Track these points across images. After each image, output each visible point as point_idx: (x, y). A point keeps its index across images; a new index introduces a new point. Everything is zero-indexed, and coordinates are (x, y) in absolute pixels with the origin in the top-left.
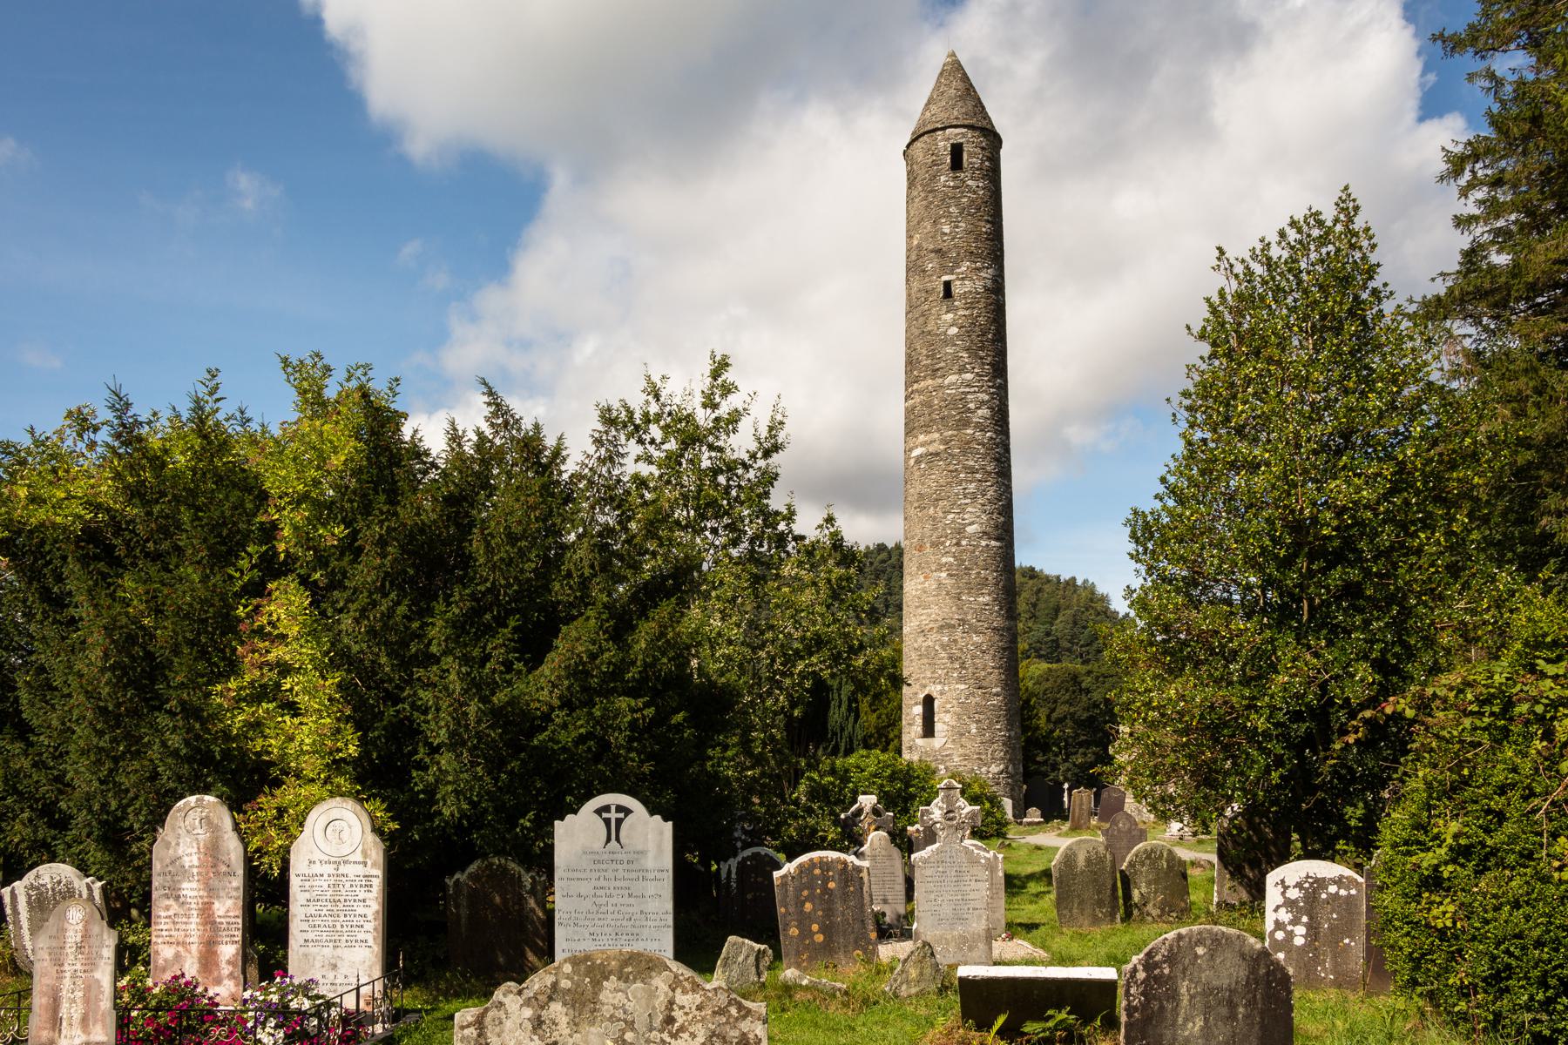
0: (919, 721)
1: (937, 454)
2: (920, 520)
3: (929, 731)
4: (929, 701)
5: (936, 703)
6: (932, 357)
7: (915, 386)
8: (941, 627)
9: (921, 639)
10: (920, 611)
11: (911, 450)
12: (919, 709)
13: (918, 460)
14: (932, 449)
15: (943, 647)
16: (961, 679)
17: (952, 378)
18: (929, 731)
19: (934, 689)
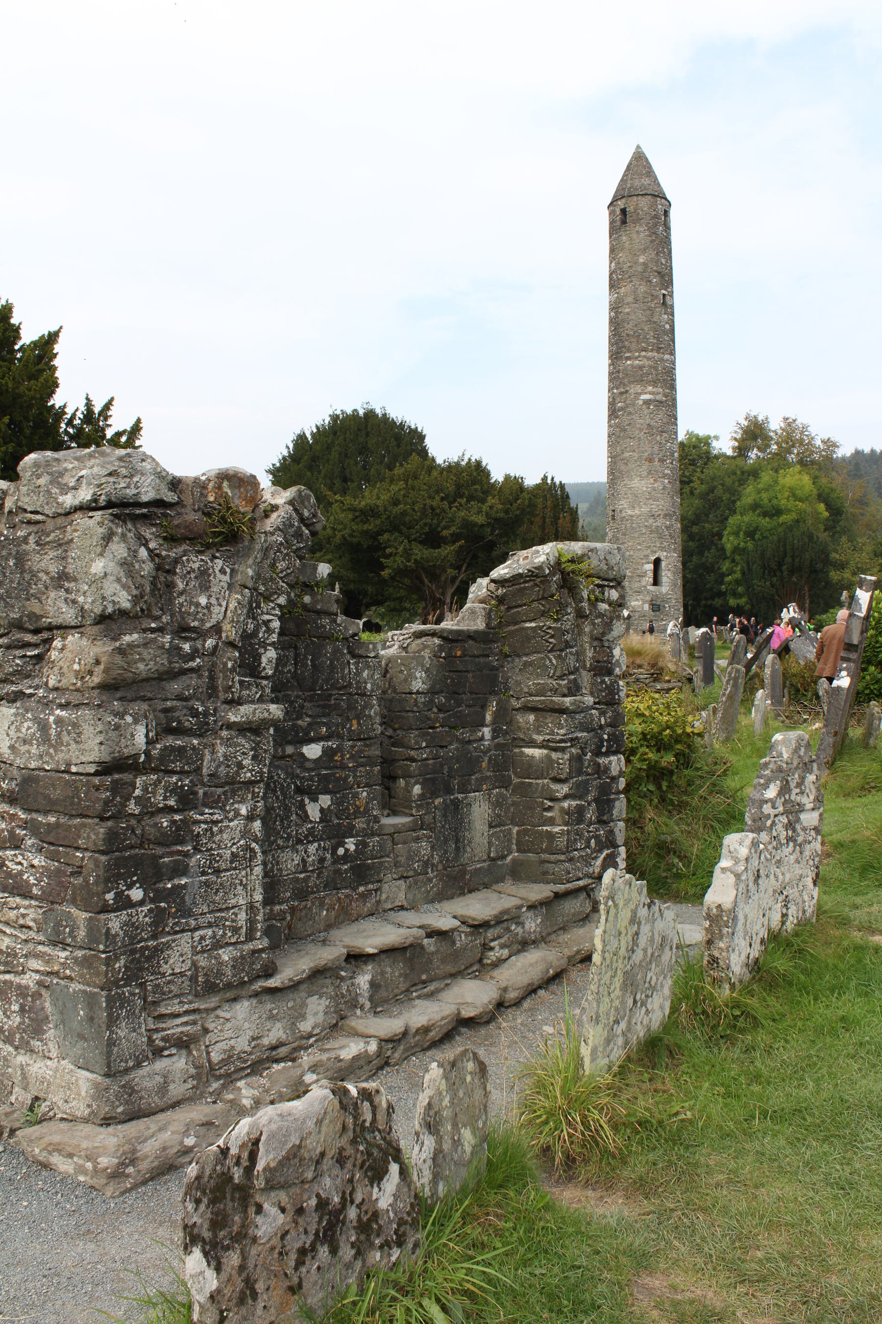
0: (651, 574)
1: (661, 402)
2: (650, 442)
3: (656, 582)
4: (657, 562)
5: (663, 564)
6: (658, 339)
7: (643, 353)
8: (666, 515)
9: (651, 521)
10: (651, 501)
11: (641, 394)
12: (651, 567)
13: (647, 403)
14: (659, 397)
15: (667, 527)
16: (675, 550)
17: (667, 357)
18: (656, 582)
19: (662, 555)
